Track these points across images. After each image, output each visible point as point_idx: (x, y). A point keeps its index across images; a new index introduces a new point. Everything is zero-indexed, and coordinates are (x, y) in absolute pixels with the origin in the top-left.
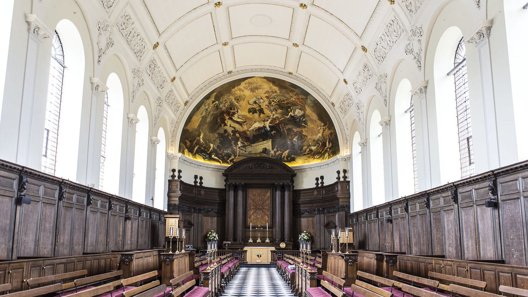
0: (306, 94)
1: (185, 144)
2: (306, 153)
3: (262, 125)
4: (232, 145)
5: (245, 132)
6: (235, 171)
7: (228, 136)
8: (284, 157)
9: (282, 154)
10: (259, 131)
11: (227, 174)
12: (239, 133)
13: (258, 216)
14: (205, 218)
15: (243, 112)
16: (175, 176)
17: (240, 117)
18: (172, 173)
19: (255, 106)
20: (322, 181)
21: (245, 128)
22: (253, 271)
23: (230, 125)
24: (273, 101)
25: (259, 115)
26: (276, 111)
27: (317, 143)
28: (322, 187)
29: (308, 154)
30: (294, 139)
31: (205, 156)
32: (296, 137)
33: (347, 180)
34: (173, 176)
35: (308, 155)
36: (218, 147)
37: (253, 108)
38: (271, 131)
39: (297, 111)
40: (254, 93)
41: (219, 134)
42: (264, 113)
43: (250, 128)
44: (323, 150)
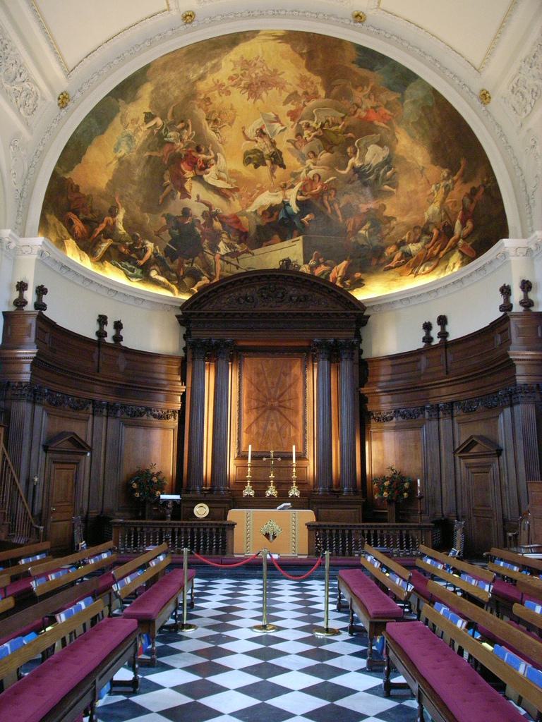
0: (404, 78)
1: (69, 224)
2: (392, 265)
3: (276, 199)
4: (202, 250)
5: (236, 219)
6: (208, 308)
7: (193, 225)
8: (336, 279)
9: (331, 270)
10: (271, 216)
11: (188, 317)
12: (222, 219)
13: (269, 427)
14: (128, 432)
15: (228, 162)
16: (26, 303)
17: (223, 175)
18: (16, 295)
19: (261, 145)
20: (443, 328)
21: (236, 206)
22: (253, 588)
23: (196, 199)
24: (308, 126)
25: (272, 171)
26: (315, 156)
27: (426, 231)
28: (445, 344)
29: (398, 266)
30: (362, 232)
31: (132, 271)
32: (368, 225)
33: (534, 309)
34: (20, 303)
35: (398, 270)
36: (167, 251)
37: (256, 151)
38: (302, 213)
39: (372, 149)
40: (259, 101)
41: (168, 217)
42: (283, 166)
43: (248, 206)
44: (441, 250)
